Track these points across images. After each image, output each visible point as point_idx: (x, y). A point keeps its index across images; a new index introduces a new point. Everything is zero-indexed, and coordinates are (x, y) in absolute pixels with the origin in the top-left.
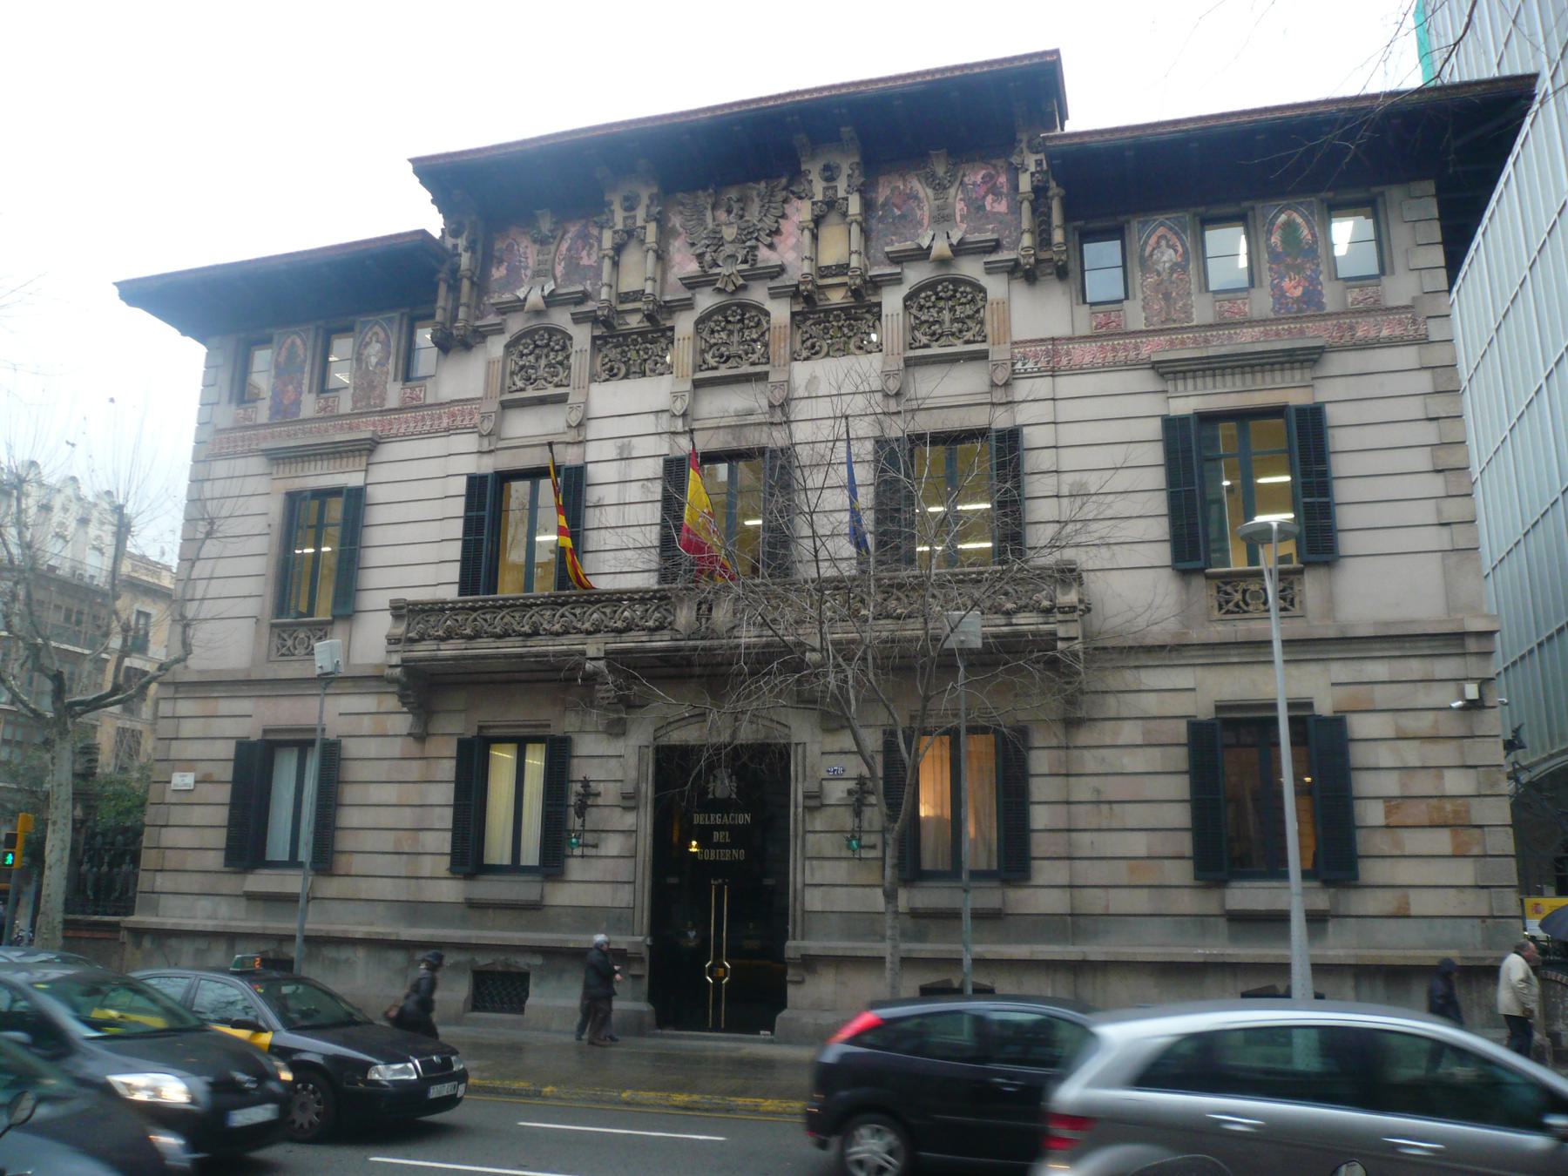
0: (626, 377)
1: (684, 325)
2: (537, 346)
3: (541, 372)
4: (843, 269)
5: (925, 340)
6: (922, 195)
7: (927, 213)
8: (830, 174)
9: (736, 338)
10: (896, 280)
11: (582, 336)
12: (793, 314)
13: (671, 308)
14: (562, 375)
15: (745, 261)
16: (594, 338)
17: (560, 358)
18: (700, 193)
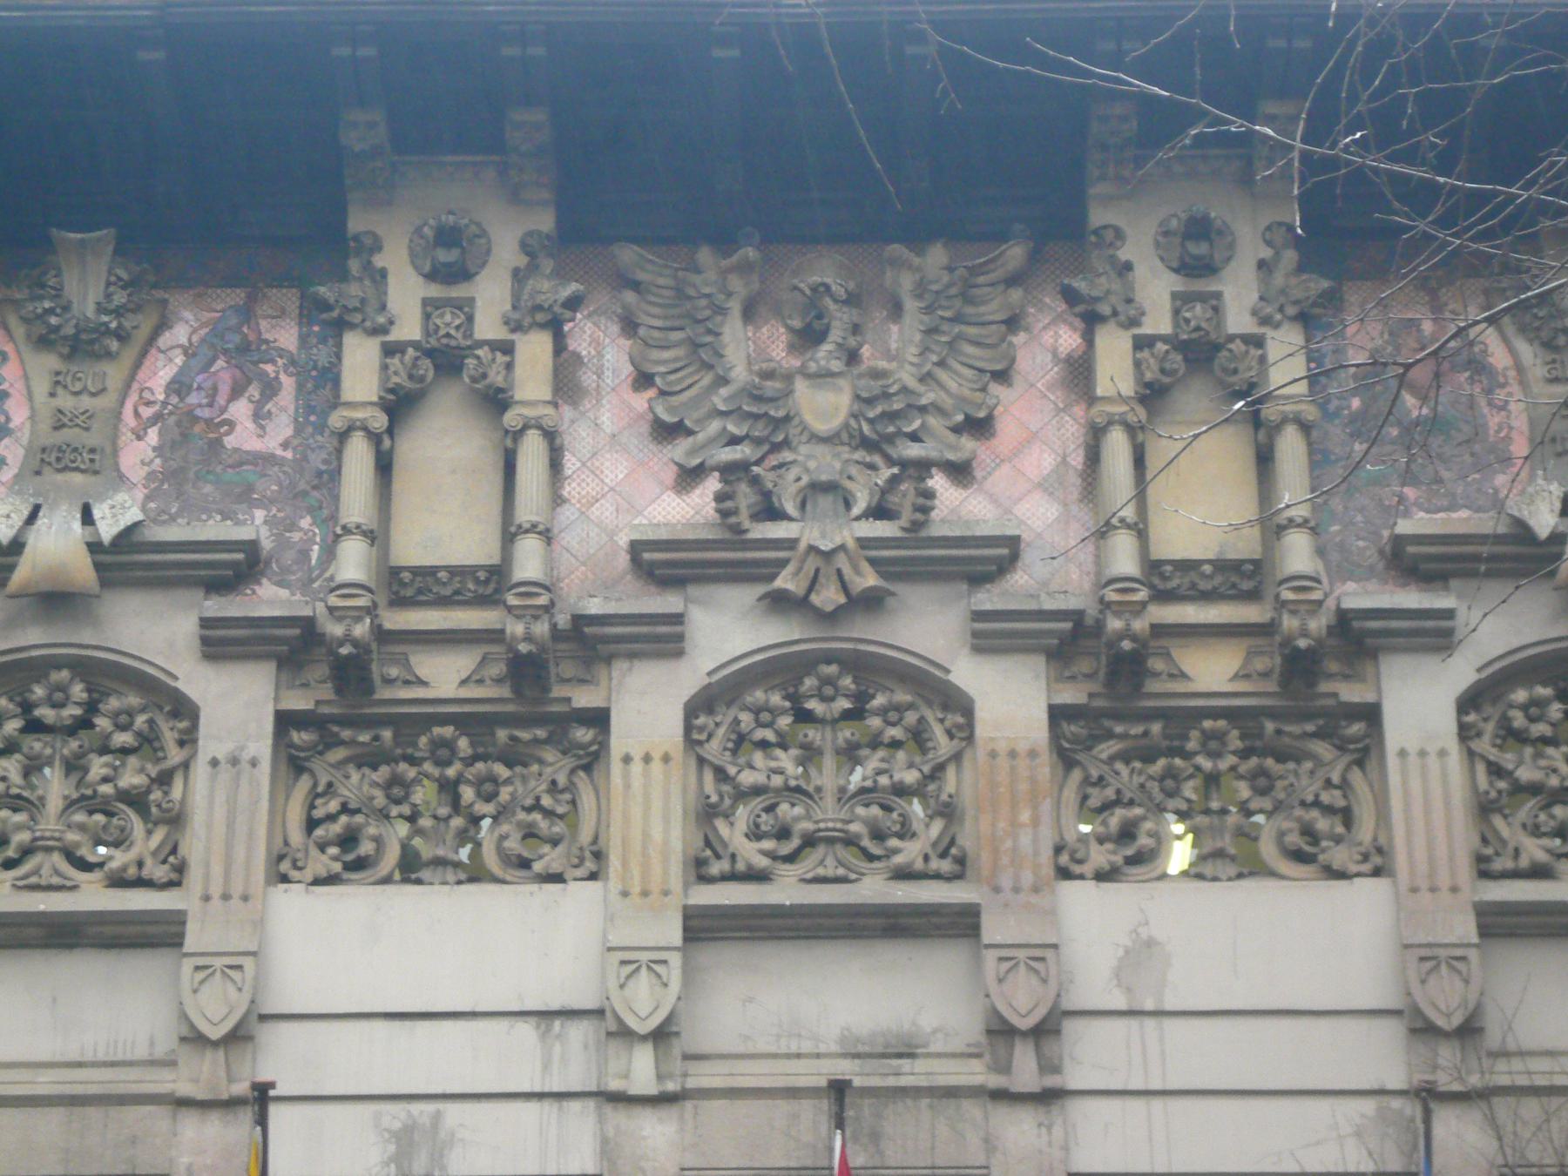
0: (410, 869)
1: (646, 709)
2: (35, 727)
3: (49, 823)
4: (1240, 577)
5: (1535, 850)
6: (1499, 357)
7: (1520, 422)
8: (1196, 252)
9: (827, 776)
10: (1435, 636)
11: (238, 709)
12: (1057, 714)
13: (593, 643)
14: (145, 842)
15: (879, 512)
16: (285, 721)
17: (131, 778)
18: (705, 255)
